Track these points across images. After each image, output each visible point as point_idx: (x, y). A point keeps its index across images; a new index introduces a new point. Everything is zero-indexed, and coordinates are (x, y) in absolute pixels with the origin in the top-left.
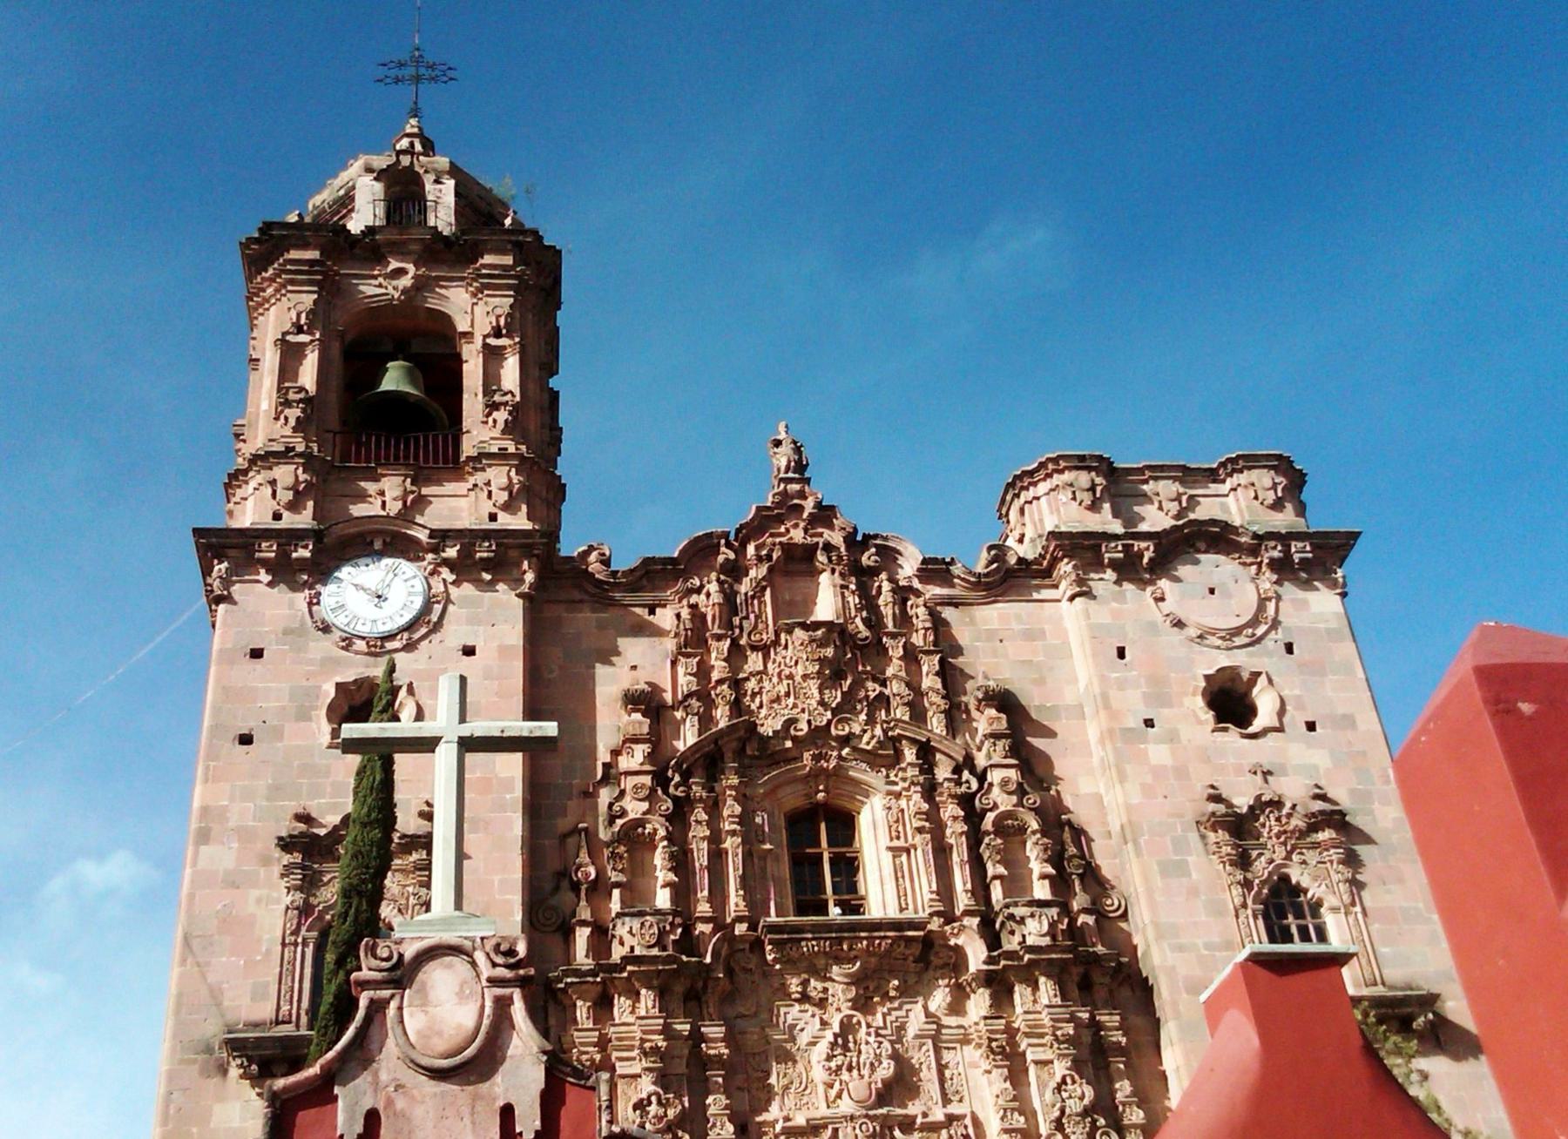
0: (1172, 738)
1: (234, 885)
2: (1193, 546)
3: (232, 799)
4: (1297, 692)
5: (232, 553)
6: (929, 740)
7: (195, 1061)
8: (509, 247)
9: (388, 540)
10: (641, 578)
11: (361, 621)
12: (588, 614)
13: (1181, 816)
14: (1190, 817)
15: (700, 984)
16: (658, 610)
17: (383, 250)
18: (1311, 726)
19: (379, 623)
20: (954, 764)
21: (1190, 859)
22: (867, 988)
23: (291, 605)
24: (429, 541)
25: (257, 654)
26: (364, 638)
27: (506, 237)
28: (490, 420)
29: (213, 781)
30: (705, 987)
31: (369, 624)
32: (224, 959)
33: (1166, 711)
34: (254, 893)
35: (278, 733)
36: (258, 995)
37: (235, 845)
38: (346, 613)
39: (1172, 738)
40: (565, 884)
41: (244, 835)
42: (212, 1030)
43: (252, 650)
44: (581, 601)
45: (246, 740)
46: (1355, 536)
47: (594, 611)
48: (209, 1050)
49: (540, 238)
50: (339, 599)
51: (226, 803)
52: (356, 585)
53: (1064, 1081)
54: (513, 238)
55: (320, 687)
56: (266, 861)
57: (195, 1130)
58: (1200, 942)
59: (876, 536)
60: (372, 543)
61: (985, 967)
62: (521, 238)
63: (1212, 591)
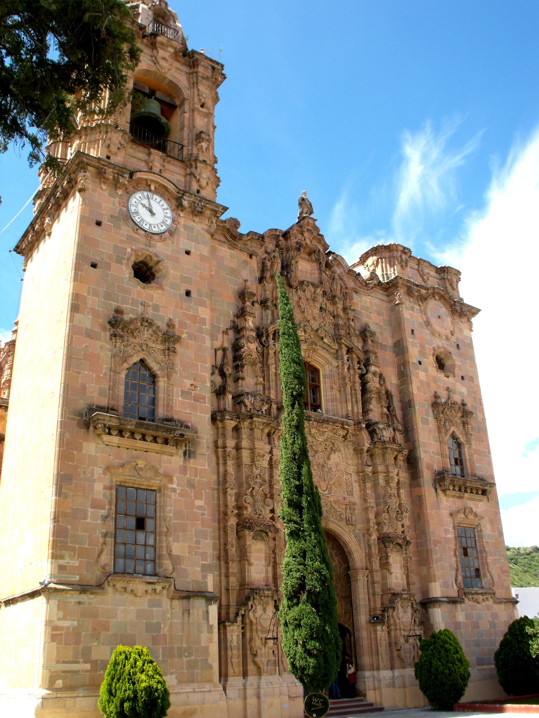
0: (426, 370)
1: (89, 336)
2: (434, 297)
3: (89, 294)
4: (459, 364)
5: (90, 168)
6: (352, 348)
7: (75, 419)
8: (210, 67)
9: (157, 187)
10: (249, 240)
11: (145, 223)
12: (227, 249)
13: (427, 401)
14: (430, 403)
15: (273, 431)
16: (254, 257)
17: (157, 45)
18: (463, 378)
19: (153, 226)
20: (358, 360)
21: (430, 419)
22: (326, 444)
23: (114, 204)
24: (177, 194)
25: (99, 224)
26: (146, 231)
27: (210, 63)
28: (199, 144)
29: (80, 282)
30: (274, 432)
31: (148, 225)
32: (86, 372)
33: (425, 359)
34: (99, 343)
35: (108, 266)
36: (101, 393)
37: (90, 317)
38: (139, 216)
39: (426, 370)
40: (217, 372)
41: (95, 313)
42: (81, 404)
43: (97, 221)
44: (224, 242)
45: (94, 266)
46: (479, 310)
47: (229, 248)
48: (81, 415)
49: (223, 69)
50: (136, 208)
51: (86, 294)
52: (142, 204)
53: (390, 496)
54: (213, 65)
55: (126, 249)
56: (104, 329)
57: (75, 453)
58: (431, 451)
59: (334, 253)
60: (150, 186)
61: (368, 446)
62: (216, 66)
63: (439, 317)
